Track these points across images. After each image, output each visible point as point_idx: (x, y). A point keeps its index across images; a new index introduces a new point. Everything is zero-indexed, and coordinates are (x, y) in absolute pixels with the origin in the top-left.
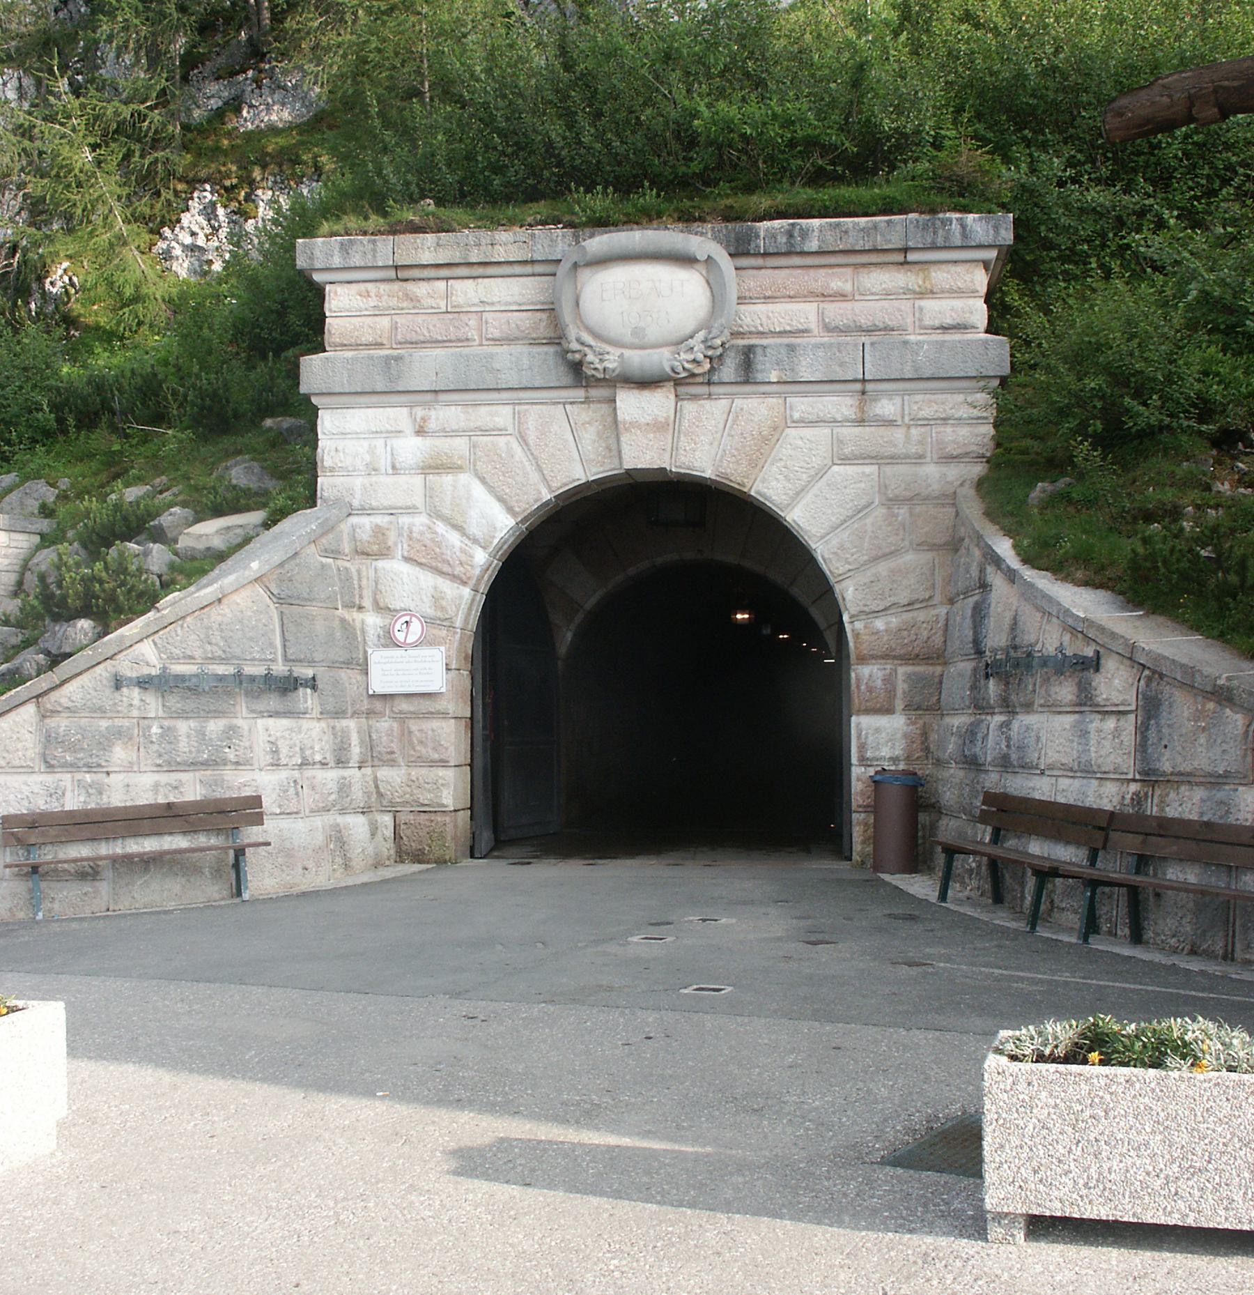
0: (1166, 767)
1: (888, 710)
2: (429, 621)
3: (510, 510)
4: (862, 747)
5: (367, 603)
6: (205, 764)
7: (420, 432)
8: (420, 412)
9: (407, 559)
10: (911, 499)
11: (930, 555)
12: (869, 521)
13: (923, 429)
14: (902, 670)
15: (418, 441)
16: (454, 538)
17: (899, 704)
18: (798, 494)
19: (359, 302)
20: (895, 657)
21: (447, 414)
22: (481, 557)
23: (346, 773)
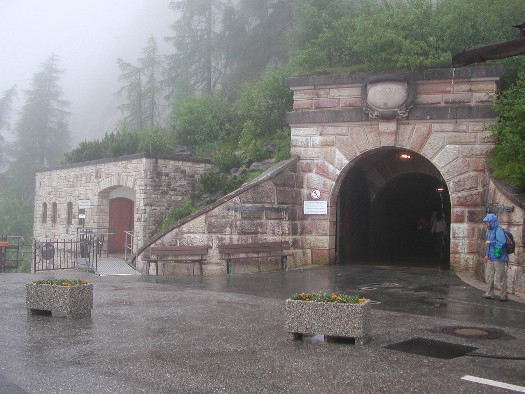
2: (322, 192)
3: (347, 158)
4: (454, 234)
5: (305, 186)
6: (253, 233)
7: (321, 135)
8: (320, 129)
9: (316, 173)
10: (471, 156)
11: (477, 173)
12: (458, 162)
13: (475, 134)
14: (467, 209)
15: (320, 137)
16: (331, 167)
18: (435, 154)
19: (303, 96)
20: (465, 206)
21: (330, 129)
22: (338, 172)
23: (296, 237)
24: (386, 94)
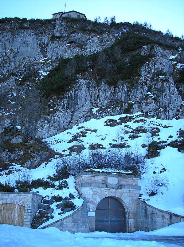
0: (173, 222)
1: (132, 219)
7: (92, 191)
16: (95, 201)
17: (133, 218)
21: (95, 189)
24: (112, 181)
